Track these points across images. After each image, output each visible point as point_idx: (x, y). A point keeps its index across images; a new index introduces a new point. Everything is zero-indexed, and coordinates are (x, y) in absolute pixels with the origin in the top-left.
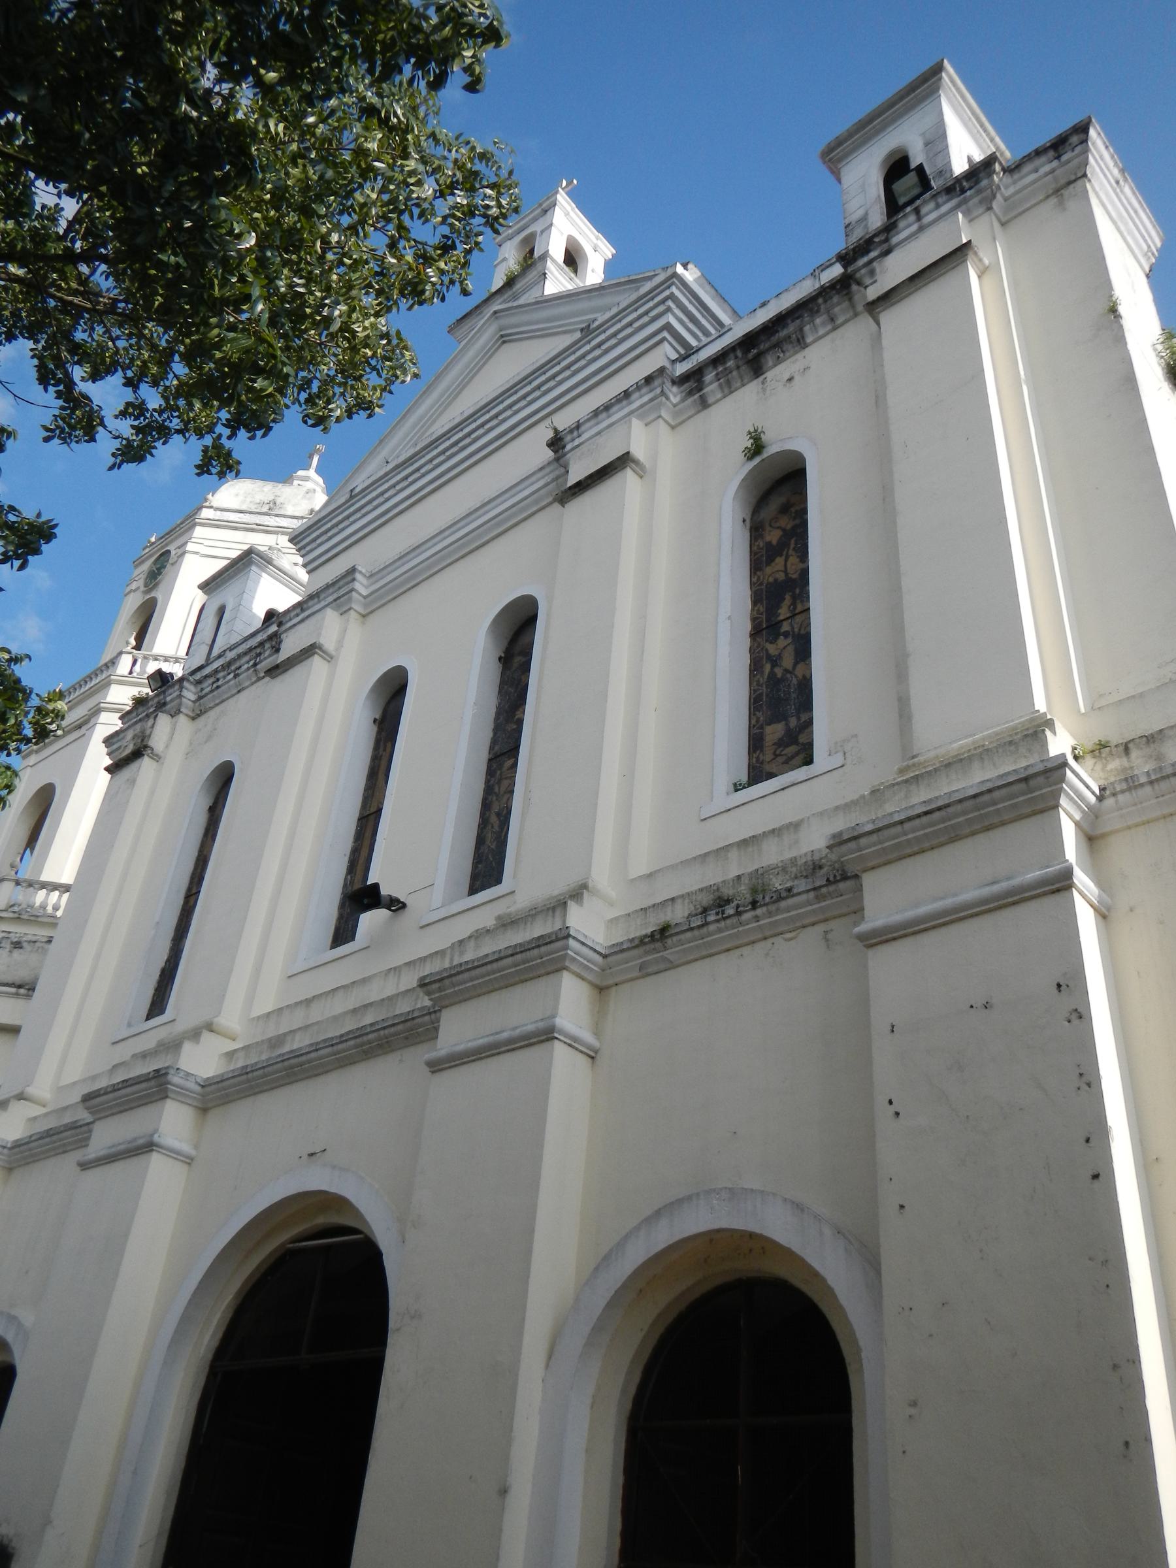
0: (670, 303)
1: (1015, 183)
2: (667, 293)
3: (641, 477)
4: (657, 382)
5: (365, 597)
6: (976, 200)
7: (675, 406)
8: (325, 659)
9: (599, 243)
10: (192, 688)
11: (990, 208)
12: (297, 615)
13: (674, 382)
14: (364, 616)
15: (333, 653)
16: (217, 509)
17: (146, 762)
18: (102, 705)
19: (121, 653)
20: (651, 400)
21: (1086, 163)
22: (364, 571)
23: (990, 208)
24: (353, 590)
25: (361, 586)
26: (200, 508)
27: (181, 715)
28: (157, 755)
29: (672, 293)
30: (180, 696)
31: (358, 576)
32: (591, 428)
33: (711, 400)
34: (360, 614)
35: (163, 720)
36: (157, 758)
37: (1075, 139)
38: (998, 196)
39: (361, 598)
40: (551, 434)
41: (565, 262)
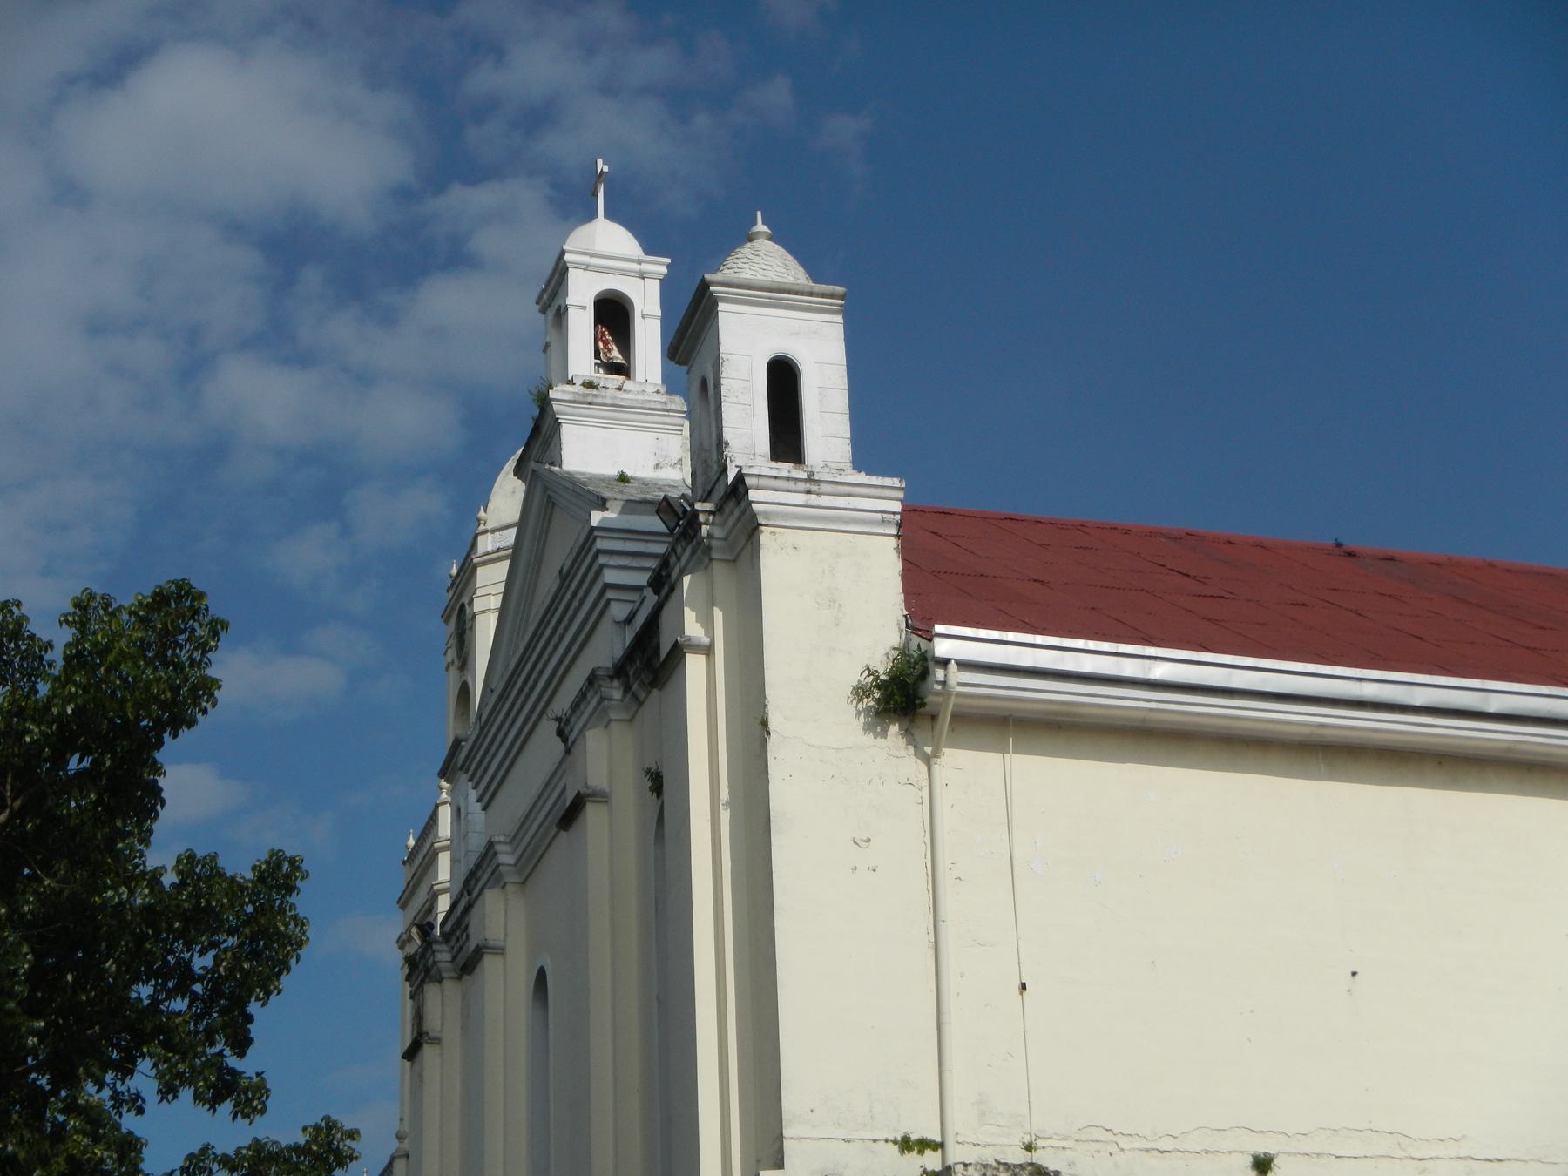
0: (602, 560)
1: (727, 519)
2: (594, 550)
3: (606, 802)
4: (596, 686)
5: (516, 865)
6: (699, 551)
7: (622, 700)
8: (496, 953)
9: (645, 267)
10: (444, 947)
11: (711, 559)
12: (476, 885)
13: (611, 678)
14: (523, 883)
15: (502, 944)
16: (493, 531)
17: (428, 1051)
18: (435, 888)
19: (437, 806)
20: (599, 703)
21: (754, 515)
22: (502, 838)
23: (711, 559)
24: (498, 866)
25: (506, 857)
26: (473, 545)
27: (445, 981)
28: (436, 1039)
29: (597, 550)
30: (435, 963)
31: (498, 848)
32: (578, 719)
33: (642, 699)
34: (518, 883)
35: (432, 991)
36: (437, 1041)
37: (741, 489)
38: (714, 543)
39: (512, 868)
40: (555, 725)
41: (646, 254)
